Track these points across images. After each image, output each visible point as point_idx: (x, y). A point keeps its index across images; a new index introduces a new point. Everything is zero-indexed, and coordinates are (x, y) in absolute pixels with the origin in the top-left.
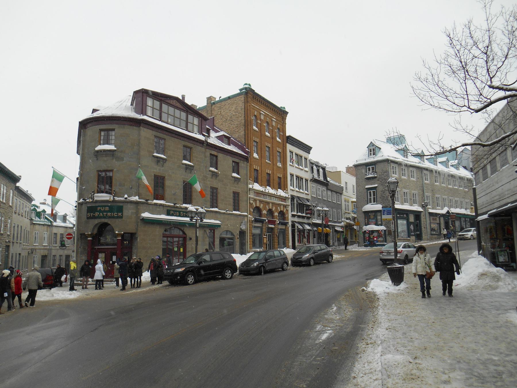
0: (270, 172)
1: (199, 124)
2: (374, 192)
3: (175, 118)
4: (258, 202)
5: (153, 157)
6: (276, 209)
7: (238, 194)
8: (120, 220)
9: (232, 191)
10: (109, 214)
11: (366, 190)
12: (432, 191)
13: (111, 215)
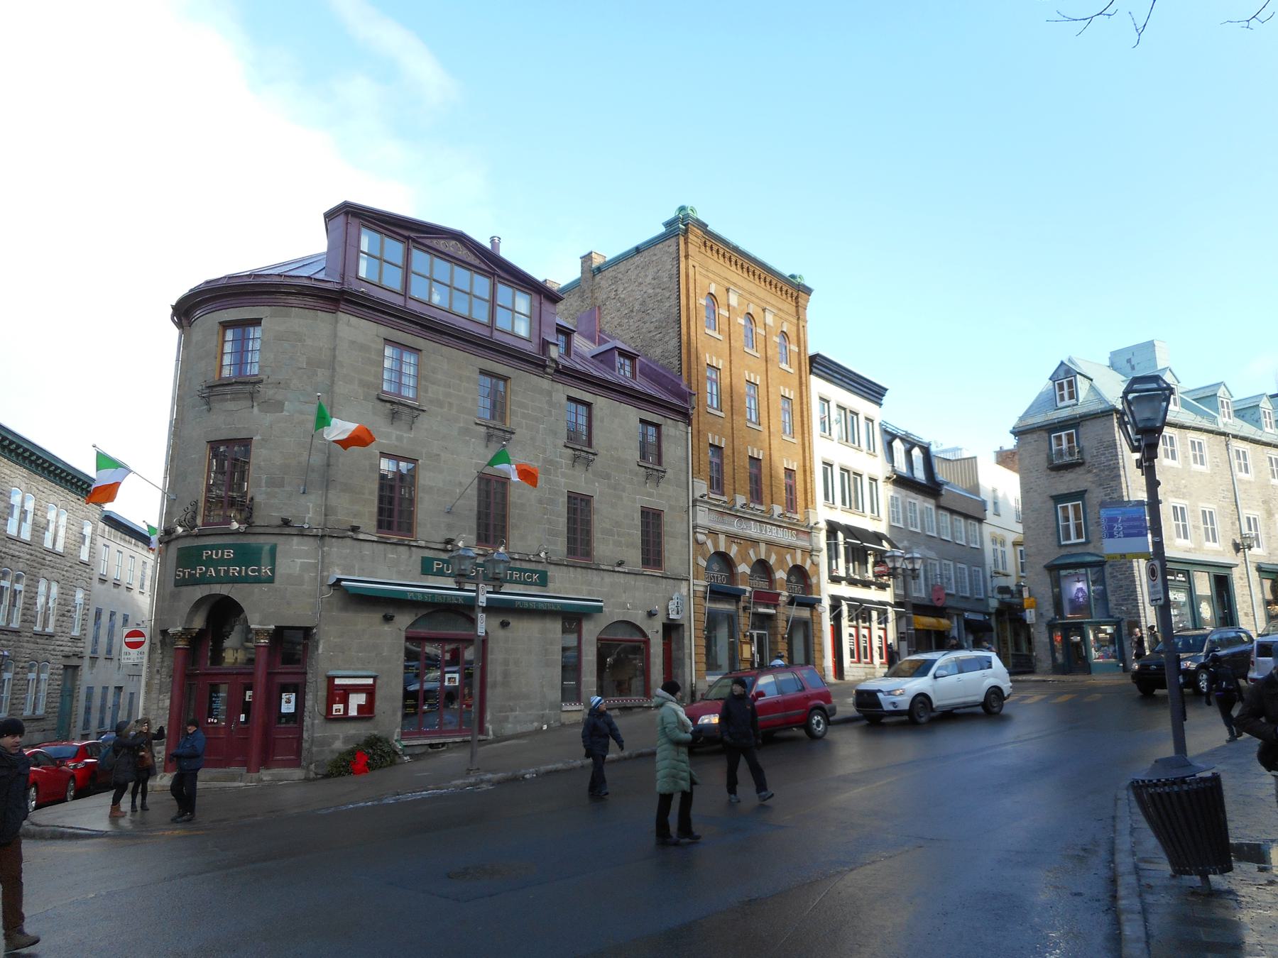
0: (758, 454)
1: (531, 313)
2: (1076, 508)
3: (455, 292)
4: (722, 538)
5: (378, 401)
6: (781, 561)
7: (657, 514)
8: (265, 587)
9: (638, 506)
10: (234, 571)
11: (1051, 503)
12: (1264, 502)
13: (240, 572)
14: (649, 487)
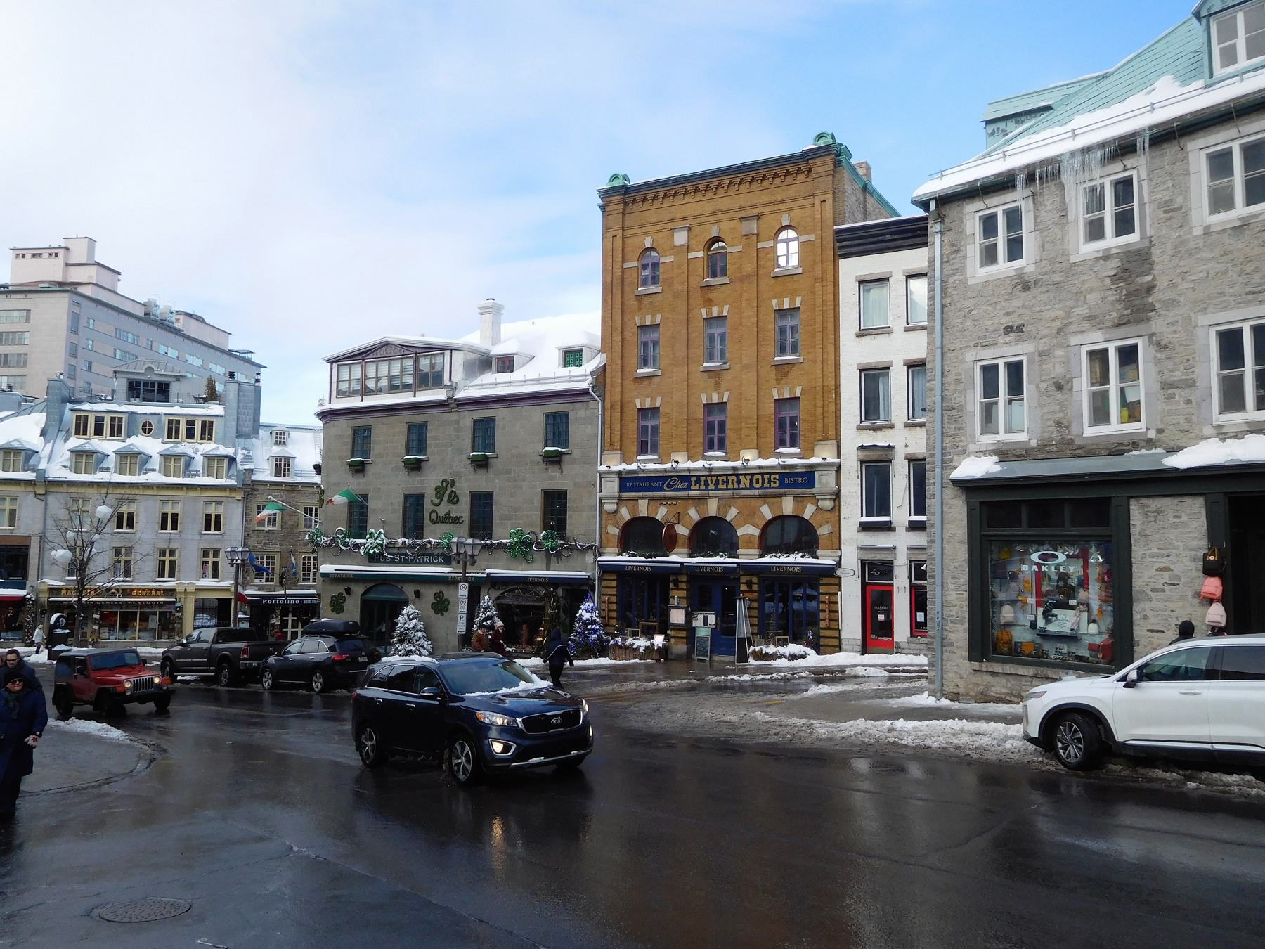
7: (562, 494)
9: (539, 490)
14: (553, 471)
